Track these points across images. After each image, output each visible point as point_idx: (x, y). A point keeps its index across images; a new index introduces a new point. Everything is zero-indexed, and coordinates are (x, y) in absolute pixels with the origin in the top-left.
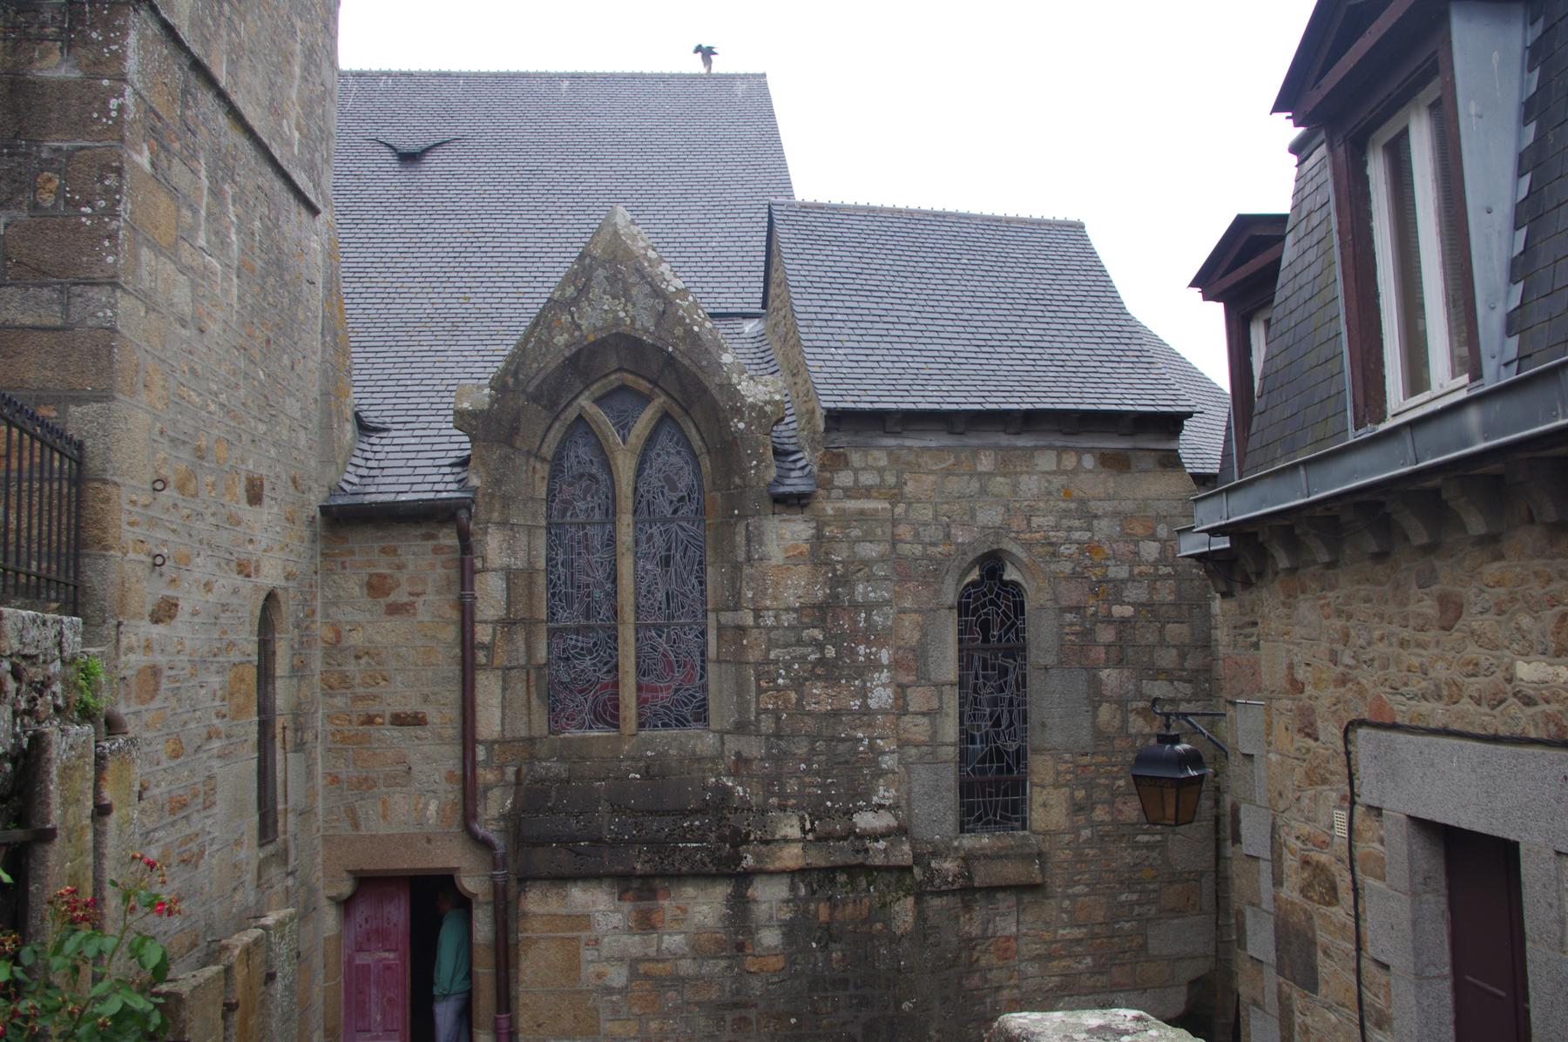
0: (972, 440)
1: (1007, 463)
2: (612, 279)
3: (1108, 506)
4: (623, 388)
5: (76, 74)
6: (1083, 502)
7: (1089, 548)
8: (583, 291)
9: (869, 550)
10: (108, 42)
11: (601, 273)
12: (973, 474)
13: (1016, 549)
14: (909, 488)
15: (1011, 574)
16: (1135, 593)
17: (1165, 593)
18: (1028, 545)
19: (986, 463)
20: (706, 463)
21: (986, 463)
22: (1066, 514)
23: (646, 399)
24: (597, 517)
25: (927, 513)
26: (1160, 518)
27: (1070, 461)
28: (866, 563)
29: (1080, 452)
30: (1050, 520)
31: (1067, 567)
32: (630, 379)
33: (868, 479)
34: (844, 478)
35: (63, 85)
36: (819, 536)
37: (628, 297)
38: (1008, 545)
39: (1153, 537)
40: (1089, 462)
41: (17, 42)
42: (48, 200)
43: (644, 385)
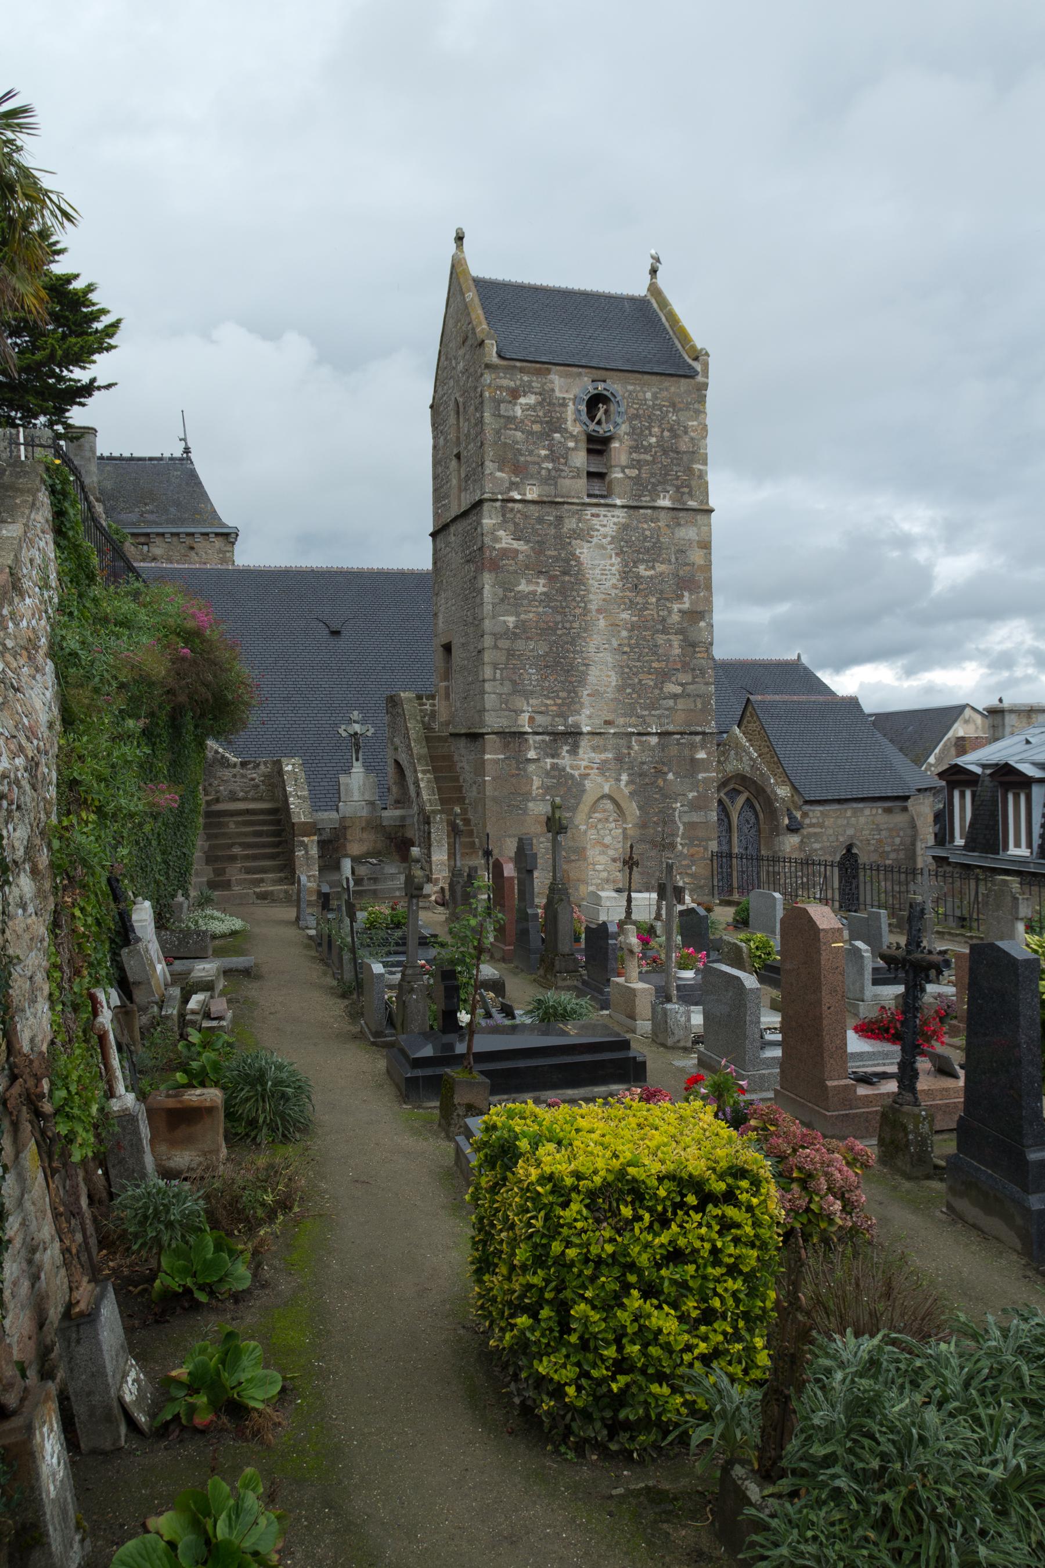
0: (845, 806)
1: (855, 811)
2: (737, 754)
3: (885, 826)
4: (734, 789)
5: (705, 756)
6: (877, 825)
7: (880, 841)
8: (727, 759)
9: (817, 846)
11: (733, 752)
12: (845, 817)
13: (858, 843)
14: (826, 823)
15: (855, 851)
16: (893, 856)
17: (902, 855)
18: (861, 841)
19: (849, 813)
20: (761, 816)
21: (849, 813)
22: (873, 829)
23: (739, 792)
24: (724, 834)
25: (831, 831)
26: (901, 829)
27: (874, 811)
28: (816, 850)
29: (877, 808)
30: (868, 832)
31: (872, 848)
32: (737, 787)
33: (814, 821)
34: (807, 821)
35: (703, 759)
36: (802, 841)
37: (741, 760)
38: (855, 841)
39: (898, 836)
40: (880, 811)
42: (701, 790)
43: (741, 788)
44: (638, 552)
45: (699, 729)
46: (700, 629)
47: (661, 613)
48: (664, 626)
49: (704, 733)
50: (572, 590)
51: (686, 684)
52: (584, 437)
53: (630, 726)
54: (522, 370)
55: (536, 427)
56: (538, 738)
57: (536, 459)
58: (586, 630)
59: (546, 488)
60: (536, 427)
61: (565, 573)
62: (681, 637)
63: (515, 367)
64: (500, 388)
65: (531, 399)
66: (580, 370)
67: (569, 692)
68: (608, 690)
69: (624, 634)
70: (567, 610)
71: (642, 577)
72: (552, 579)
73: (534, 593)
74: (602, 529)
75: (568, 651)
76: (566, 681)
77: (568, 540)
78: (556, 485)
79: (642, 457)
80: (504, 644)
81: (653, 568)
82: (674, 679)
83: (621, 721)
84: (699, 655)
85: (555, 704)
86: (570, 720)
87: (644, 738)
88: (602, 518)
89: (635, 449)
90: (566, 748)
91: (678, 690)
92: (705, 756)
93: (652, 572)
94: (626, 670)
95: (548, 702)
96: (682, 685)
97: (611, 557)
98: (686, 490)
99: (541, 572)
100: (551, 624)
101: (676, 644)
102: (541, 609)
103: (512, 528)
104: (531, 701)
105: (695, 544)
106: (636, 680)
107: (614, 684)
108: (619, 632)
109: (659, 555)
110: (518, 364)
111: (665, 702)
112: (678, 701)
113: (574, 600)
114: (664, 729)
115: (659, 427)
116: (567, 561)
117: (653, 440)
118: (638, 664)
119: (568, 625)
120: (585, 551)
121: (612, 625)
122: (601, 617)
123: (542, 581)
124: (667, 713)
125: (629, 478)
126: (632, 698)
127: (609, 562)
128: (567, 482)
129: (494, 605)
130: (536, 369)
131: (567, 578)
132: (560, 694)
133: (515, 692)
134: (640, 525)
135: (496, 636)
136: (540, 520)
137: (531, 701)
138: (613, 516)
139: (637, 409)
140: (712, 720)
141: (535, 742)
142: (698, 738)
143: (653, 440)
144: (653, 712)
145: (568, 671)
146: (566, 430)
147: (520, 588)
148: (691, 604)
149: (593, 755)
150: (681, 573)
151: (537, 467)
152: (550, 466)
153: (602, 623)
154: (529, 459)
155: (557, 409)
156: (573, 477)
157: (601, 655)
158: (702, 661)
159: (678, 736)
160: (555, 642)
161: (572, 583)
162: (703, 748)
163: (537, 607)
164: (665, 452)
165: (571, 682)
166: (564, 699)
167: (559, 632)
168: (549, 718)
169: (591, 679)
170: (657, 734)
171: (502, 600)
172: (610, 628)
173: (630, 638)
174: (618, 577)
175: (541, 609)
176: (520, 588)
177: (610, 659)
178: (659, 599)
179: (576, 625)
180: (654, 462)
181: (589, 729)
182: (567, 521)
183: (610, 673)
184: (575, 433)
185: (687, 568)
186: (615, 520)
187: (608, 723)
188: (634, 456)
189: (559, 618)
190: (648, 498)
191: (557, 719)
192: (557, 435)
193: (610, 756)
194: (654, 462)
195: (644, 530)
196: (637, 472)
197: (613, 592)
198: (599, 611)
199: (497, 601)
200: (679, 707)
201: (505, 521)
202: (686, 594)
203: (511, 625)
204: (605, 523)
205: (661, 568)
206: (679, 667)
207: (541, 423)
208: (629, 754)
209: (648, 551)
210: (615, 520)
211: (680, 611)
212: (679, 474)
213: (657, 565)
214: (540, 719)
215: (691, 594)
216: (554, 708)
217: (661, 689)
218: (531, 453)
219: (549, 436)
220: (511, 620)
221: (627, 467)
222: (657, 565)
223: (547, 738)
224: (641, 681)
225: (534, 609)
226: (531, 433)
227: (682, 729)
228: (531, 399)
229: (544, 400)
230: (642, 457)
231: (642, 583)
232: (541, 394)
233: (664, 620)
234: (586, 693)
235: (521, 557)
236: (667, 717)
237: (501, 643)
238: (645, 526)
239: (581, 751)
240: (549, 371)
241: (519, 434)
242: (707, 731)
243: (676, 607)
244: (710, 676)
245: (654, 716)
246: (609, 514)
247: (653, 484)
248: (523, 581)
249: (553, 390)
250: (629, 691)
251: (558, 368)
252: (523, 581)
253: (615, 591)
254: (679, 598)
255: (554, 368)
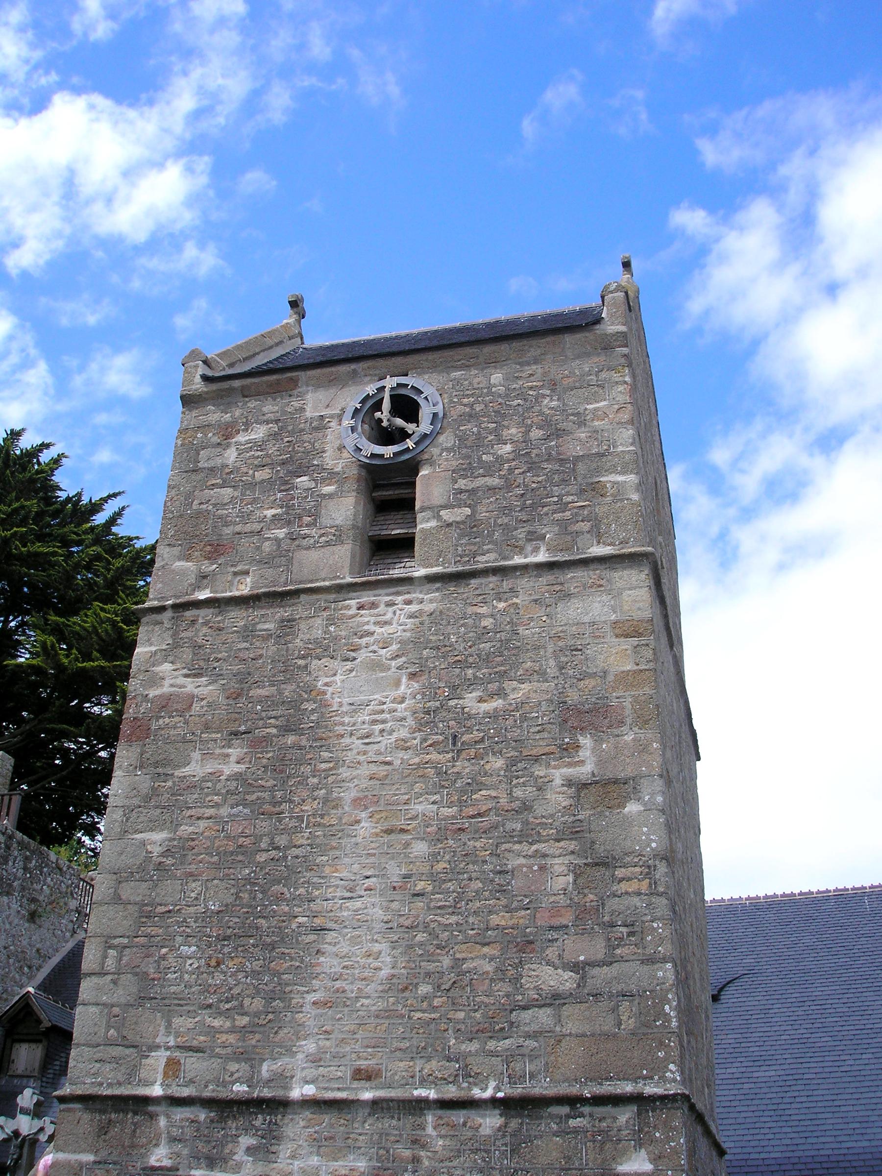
5: (648, 1167)
10: (669, 1139)
41: (603, 1143)
44: (463, 664)
45: (629, 1088)
46: (628, 822)
47: (518, 793)
48: (526, 823)
49: (637, 1099)
50: (300, 762)
51: (588, 964)
52: (354, 471)
53: (424, 1082)
54: (246, 393)
55: (262, 475)
56: (181, 1114)
57: (257, 527)
58: (324, 850)
59: (270, 573)
60: (262, 475)
61: (286, 729)
62: (572, 845)
63: (232, 390)
64: (204, 427)
65: (259, 433)
66: (353, 366)
67: (270, 998)
68: (370, 989)
69: (420, 848)
70: (285, 806)
71: (470, 717)
72: (260, 743)
73: (214, 776)
74: (379, 630)
75: (279, 898)
76: (265, 968)
77: (301, 662)
78: (290, 561)
79: (480, 482)
80: (130, 891)
81: (500, 693)
82: (551, 953)
83: (399, 1068)
84: (624, 887)
85: (232, 1030)
86: (265, 1069)
87: (458, 1116)
88: (382, 608)
89: (466, 471)
90: (246, 1141)
91: (566, 980)
92: (648, 1167)
93: (498, 703)
94: (421, 937)
95: (217, 1023)
96: (575, 967)
97: (398, 684)
98: (585, 526)
99: (236, 734)
100: (247, 841)
101: (559, 865)
102: (225, 811)
103: (187, 654)
104: (177, 1021)
105: (607, 628)
106: (446, 962)
107: (385, 973)
108: (407, 845)
109: (515, 666)
110: (237, 383)
111: (526, 1015)
112: (566, 1011)
113: (303, 782)
114: (518, 1091)
115: (520, 425)
116: (295, 704)
117: (508, 448)
118: (453, 919)
119: (281, 840)
120: (338, 678)
121: (389, 832)
122: (363, 815)
123: (235, 752)
124: (532, 1043)
125: (449, 525)
126: (435, 1009)
127: (394, 694)
128: (314, 555)
129: (128, 811)
130: (270, 385)
131: (291, 739)
132: (247, 1002)
133: (142, 999)
134: (470, 610)
135: (120, 876)
136: (248, 633)
137: (177, 1021)
138: (409, 602)
139: (471, 406)
140: (667, 1060)
141: (171, 1124)
142: (625, 1116)
143: (508, 448)
144: (491, 1045)
145: (273, 947)
146: (321, 468)
147: (186, 771)
148: (600, 763)
149: (315, 1160)
150: (573, 697)
151: (255, 539)
152: (281, 533)
153: (366, 828)
154: (238, 528)
155: (306, 437)
156: (328, 544)
157: (358, 904)
158: (636, 900)
159: (565, 1110)
160: (248, 880)
161: (301, 748)
162: (640, 1144)
163: (217, 805)
164: (533, 467)
165: (278, 974)
166: (257, 1015)
167: (261, 858)
168: (216, 1063)
169: (328, 963)
170: (494, 1102)
171: (147, 798)
172: (386, 838)
173: (435, 857)
174: (410, 722)
175: (225, 811)
176: (186, 771)
177: (378, 913)
178: (512, 763)
179: (301, 839)
180: (509, 486)
181: (310, 1090)
182: (303, 626)
183: (377, 947)
184: (338, 469)
185: (590, 683)
186: (414, 608)
187: (363, 1075)
188: (462, 483)
189: (264, 825)
190: (492, 556)
191: (233, 1066)
192: (303, 481)
193: (362, 1165)
194: (509, 486)
195: (480, 616)
196: (468, 511)
197: (398, 758)
198: (356, 802)
199: (136, 801)
200: (571, 1027)
201: (176, 645)
202: (586, 741)
203: (156, 850)
204: (389, 616)
205: (518, 691)
206: (567, 919)
207: (271, 465)
208: (416, 1160)
209: (487, 659)
210: (414, 608)
211: (569, 783)
212: (570, 499)
213: (508, 685)
214: (193, 1064)
215: (598, 741)
216: (231, 1038)
217: (516, 980)
218: (245, 518)
219: (286, 483)
220: (158, 838)
221: (445, 507)
222: (508, 685)
223: (202, 1115)
224: (457, 962)
225: (211, 812)
226: (252, 485)
227: (574, 1090)
228: (259, 433)
229: (281, 429)
230: (480, 482)
231: (469, 730)
232: (277, 421)
233: (526, 807)
234: (311, 998)
235: (196, 707)
236: (533, 1057)
237: (127, 891)
238: (484, 610)
239: (285, 1150)
240: (294, 383)
241: (229, 490)
242: (650, 1090)
243: (559, 774)
244: (662, 940)
245: (493, 1054)
246: (400, 599)
247: (506, 528)
248: (196, 755)
249: (302, 410)
250: (424, 989)
251: (310, 373)
252: (196, 755)
253: (401, 754)
254: (569, 750)
255: (302, 375)
